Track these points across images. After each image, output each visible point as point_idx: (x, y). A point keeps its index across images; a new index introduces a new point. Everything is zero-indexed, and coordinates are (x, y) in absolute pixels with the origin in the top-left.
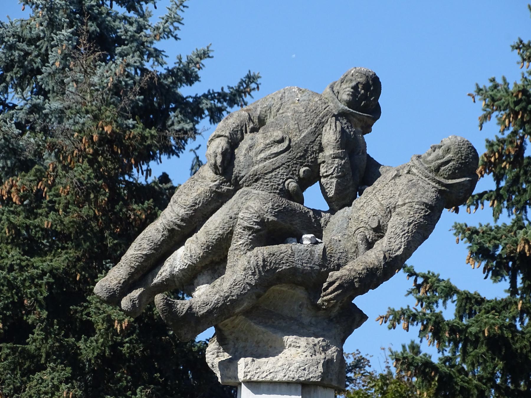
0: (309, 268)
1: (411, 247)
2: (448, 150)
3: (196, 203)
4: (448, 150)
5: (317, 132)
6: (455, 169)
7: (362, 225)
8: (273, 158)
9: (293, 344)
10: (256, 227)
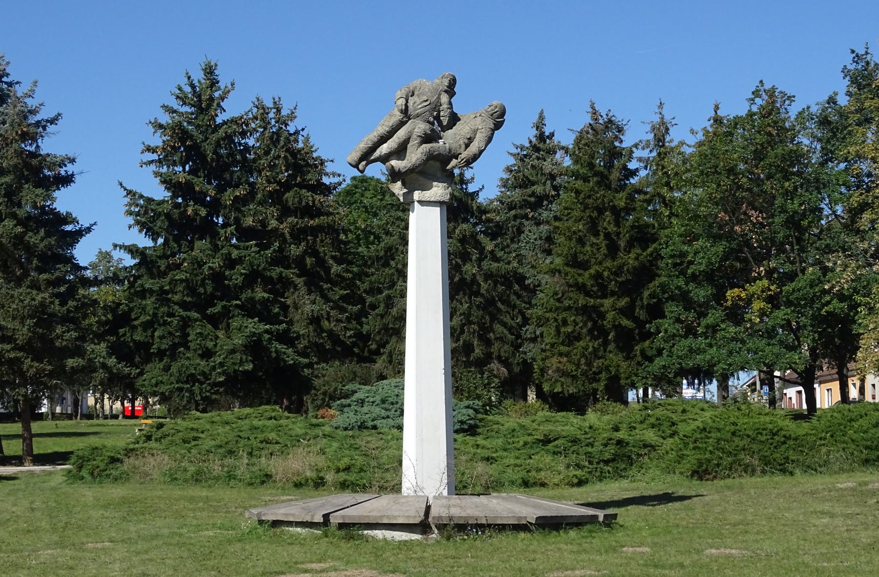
2: (496, 107)
5: (439, 98)
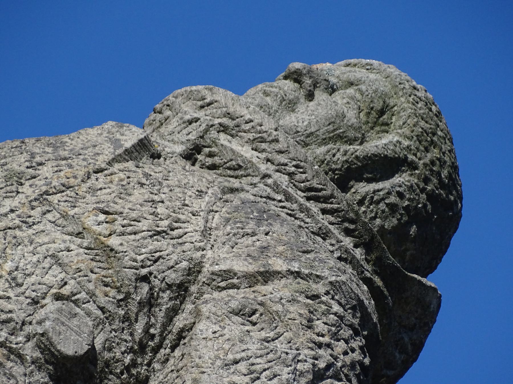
6: (414, 214)
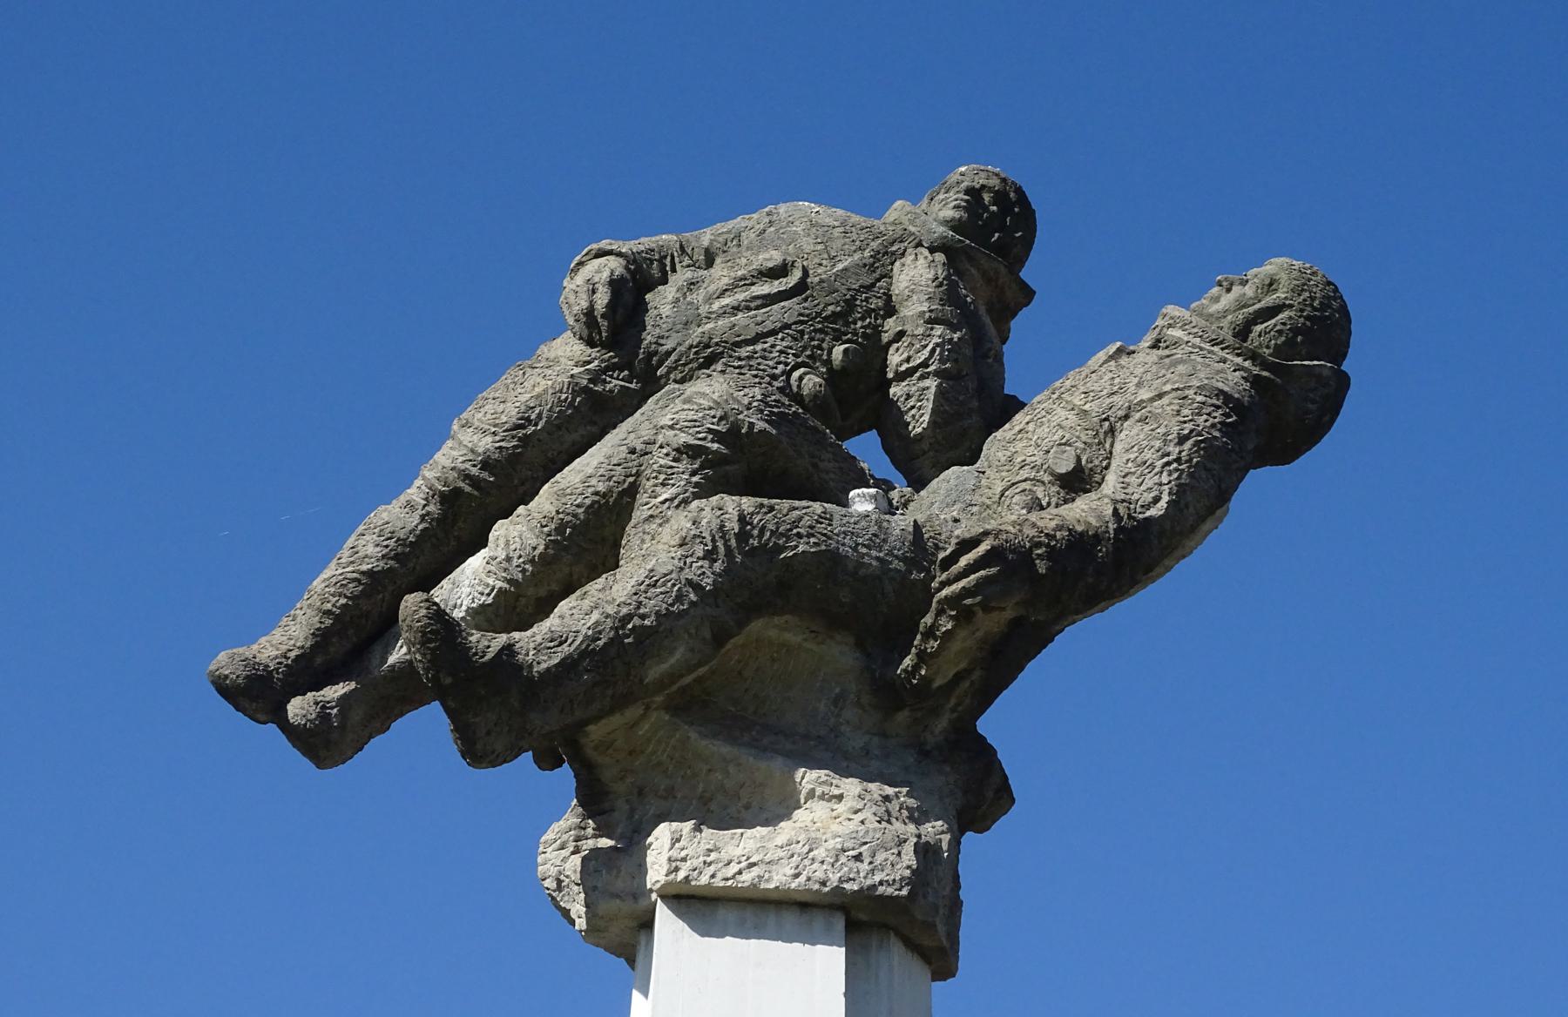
0: (874, 563)
1: (1187, 506)
3: (528, 419)
4: (1271, 285)
6: (1296, 330)
7: (1024, 474)
8: (757, 308)
9: (819, 791)
10: (716, 446)
